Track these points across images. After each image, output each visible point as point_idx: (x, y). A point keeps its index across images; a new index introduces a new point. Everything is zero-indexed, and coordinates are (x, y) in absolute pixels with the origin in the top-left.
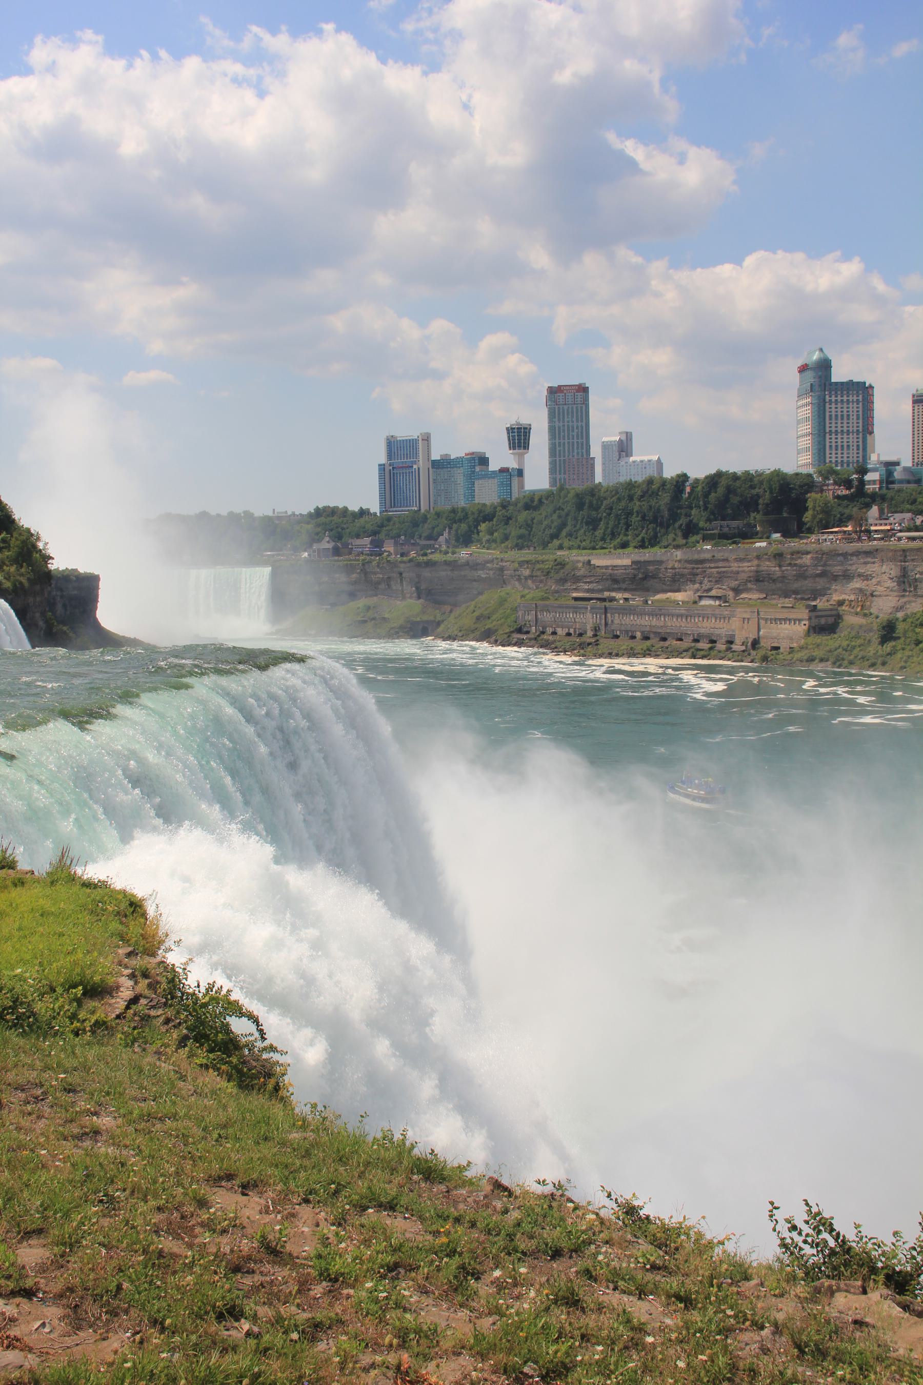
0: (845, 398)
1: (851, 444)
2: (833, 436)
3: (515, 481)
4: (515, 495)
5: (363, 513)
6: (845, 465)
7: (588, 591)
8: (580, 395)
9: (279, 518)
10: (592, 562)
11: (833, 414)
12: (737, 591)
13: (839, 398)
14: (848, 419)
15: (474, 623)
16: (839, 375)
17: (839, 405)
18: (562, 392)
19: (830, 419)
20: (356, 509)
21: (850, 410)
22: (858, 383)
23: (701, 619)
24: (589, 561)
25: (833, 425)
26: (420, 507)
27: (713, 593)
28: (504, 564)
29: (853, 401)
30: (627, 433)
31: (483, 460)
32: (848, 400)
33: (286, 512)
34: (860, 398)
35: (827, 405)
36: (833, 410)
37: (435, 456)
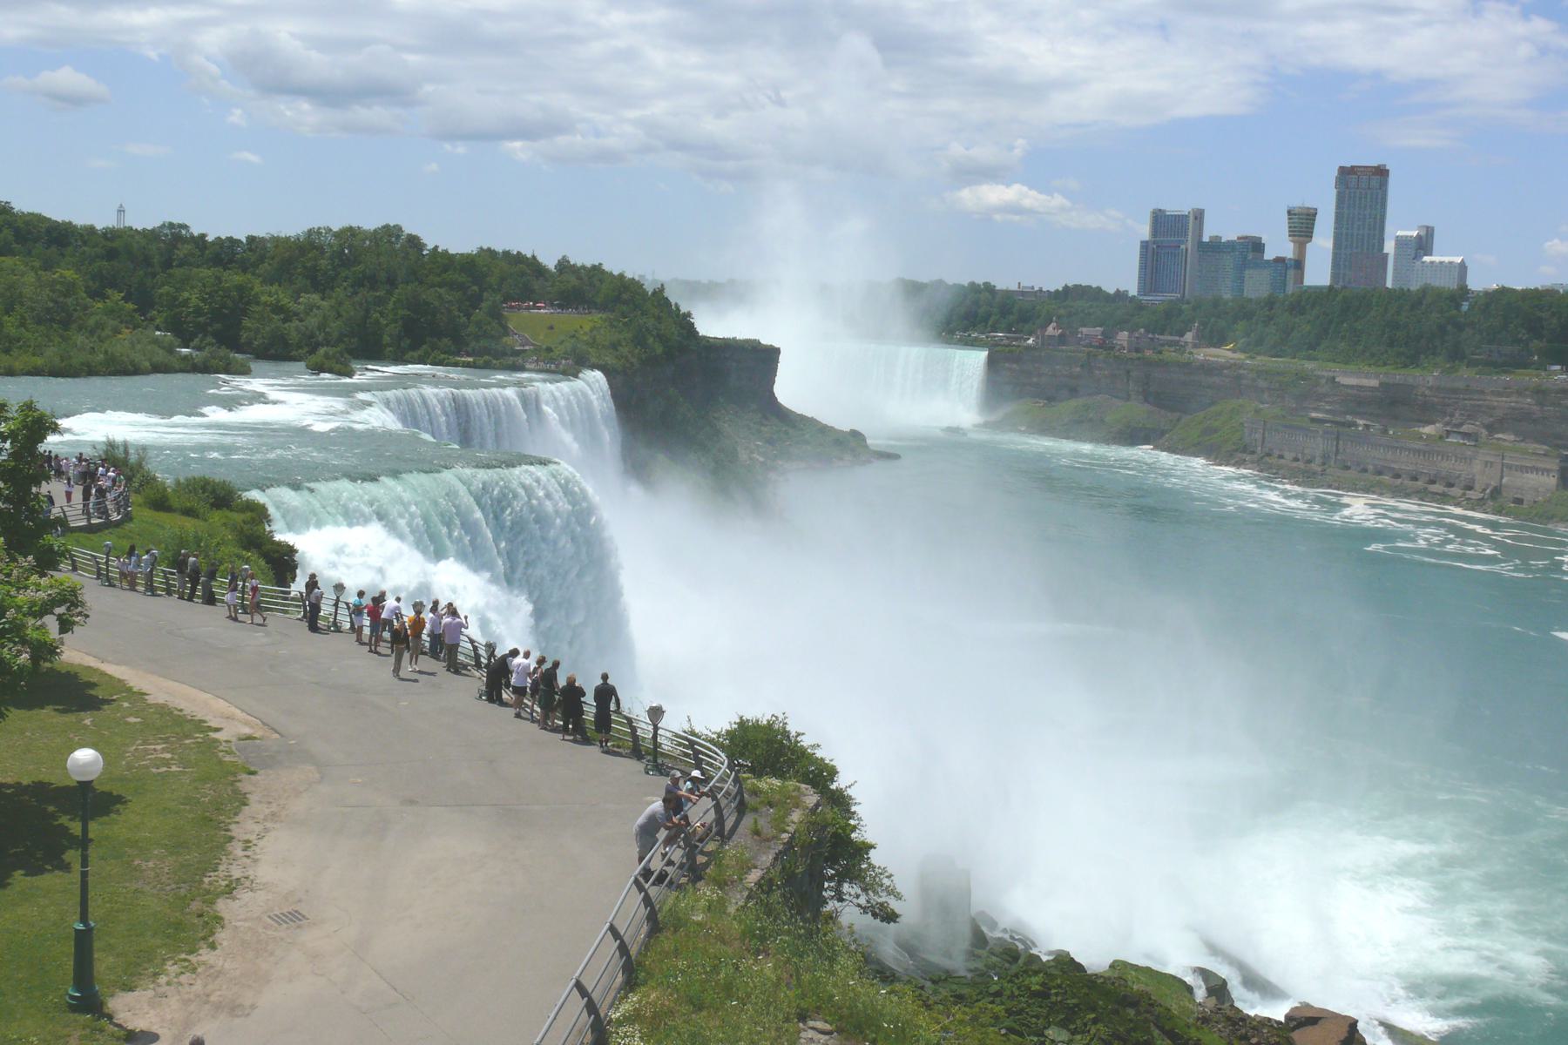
3: (1291, 273)
4: (1290, 289)
5: (1120, 296)
7: (1327, 412)
8: (1375, 181)
9: (1023, 293)
10: (1337, 380)
12: (1491, 429)
15: (1199, 437)
18: (1355, 173)
20: (1111, 291)
23: (1440, 458)
24: (1334, 378)
26: (1184, 294)
27: (1465, 428)
28: (1241, 372)
30: (1428, 227)
31: (1257, 246)
33: (1033, 288)
37: (1206, 239)
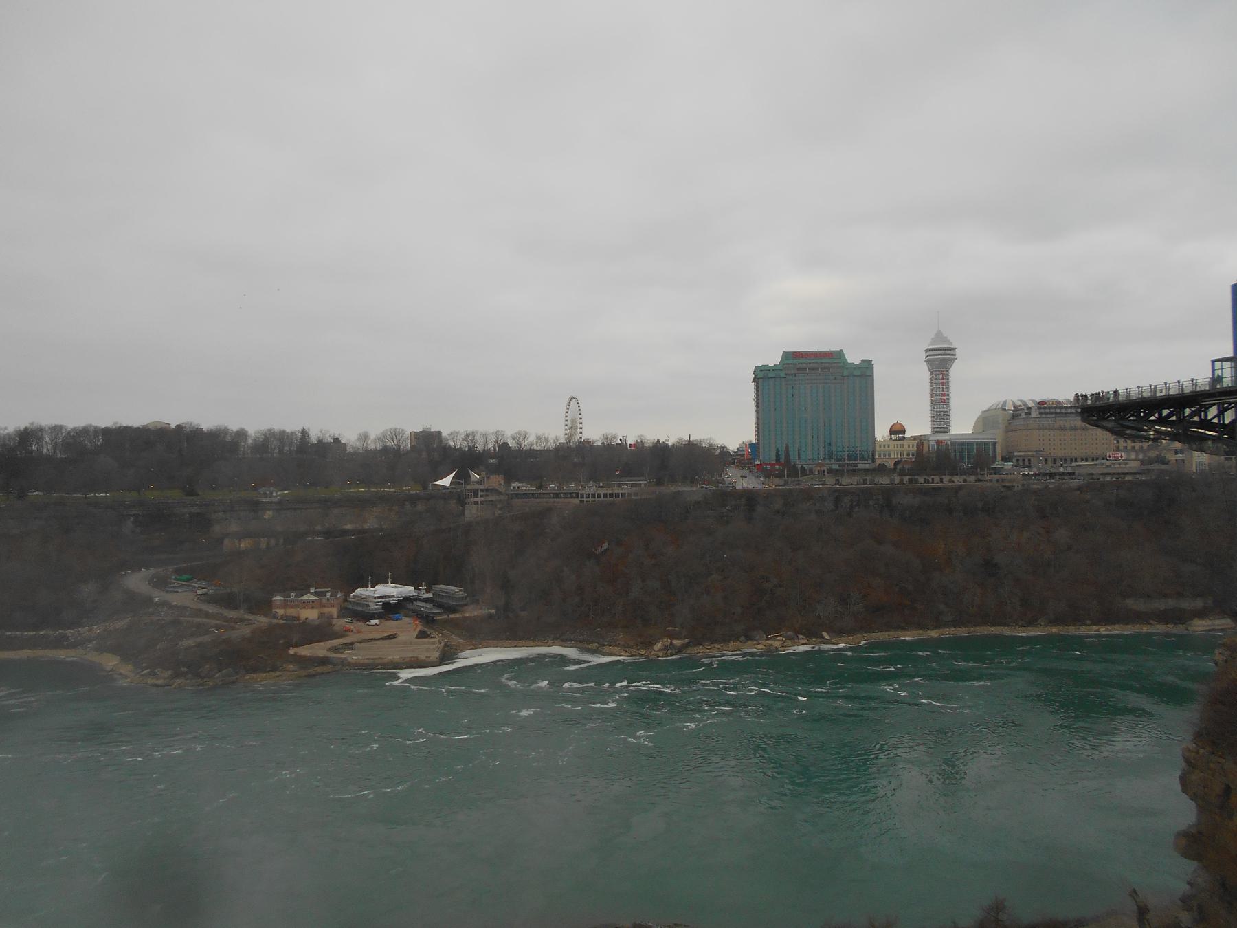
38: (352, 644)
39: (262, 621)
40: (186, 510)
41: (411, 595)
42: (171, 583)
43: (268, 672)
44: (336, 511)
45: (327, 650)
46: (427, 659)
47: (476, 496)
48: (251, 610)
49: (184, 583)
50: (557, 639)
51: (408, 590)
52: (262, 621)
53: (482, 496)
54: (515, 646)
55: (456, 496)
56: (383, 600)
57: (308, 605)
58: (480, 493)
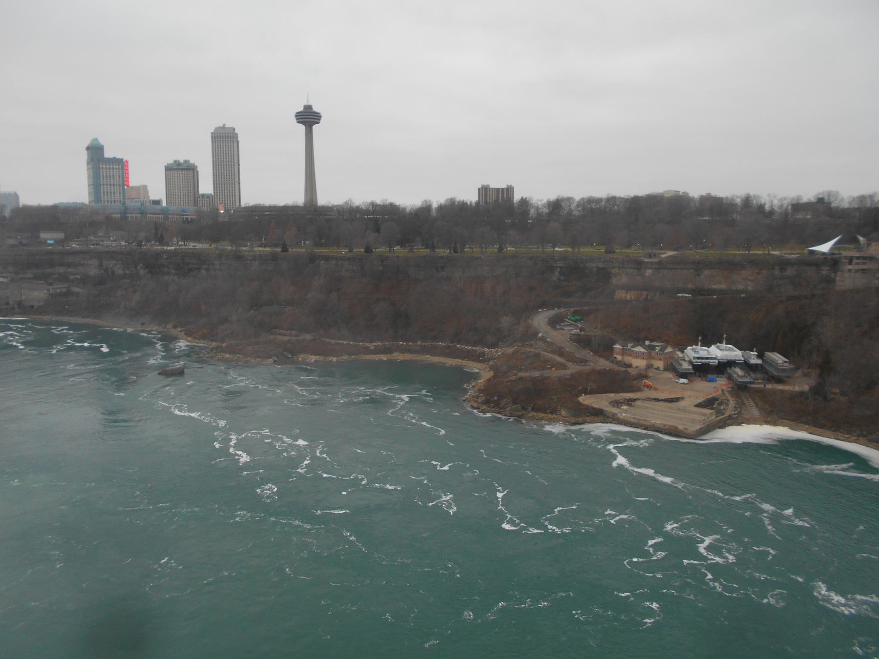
0: (111, 167)
1: (116, 191)
2: (105, 186)
6: (113, 202)
11: (105, 175)
13: (108, 166)
14: (114, 178)
16: (108, 154)
17: (108, 170)
19: (103, 177)
21: (115, 173)
22: (118, 159)
25: (105, 181)
29: (116, 169)
32: (113, 168)
34: (120, 167)
35: (101, 170)
36: (105, 172)
38: (635, 400)
39: (603, 364)
40: (594, 265)
41: (737, 359)
42: (565, 321)
43: (547, 413)
44: (707, 272)
45: (610, 403)
46: (685, 431)
47: (850, 262)
48: (596, 352)
49: (573, 323)
50: (864, 436)
51: (736, 354)
52: (603, 364)
53: (857, 264)
54: (811, 433)
55: (832, 261)
56: (703, 361)
57: (638, 356)
58: (855, 261)
